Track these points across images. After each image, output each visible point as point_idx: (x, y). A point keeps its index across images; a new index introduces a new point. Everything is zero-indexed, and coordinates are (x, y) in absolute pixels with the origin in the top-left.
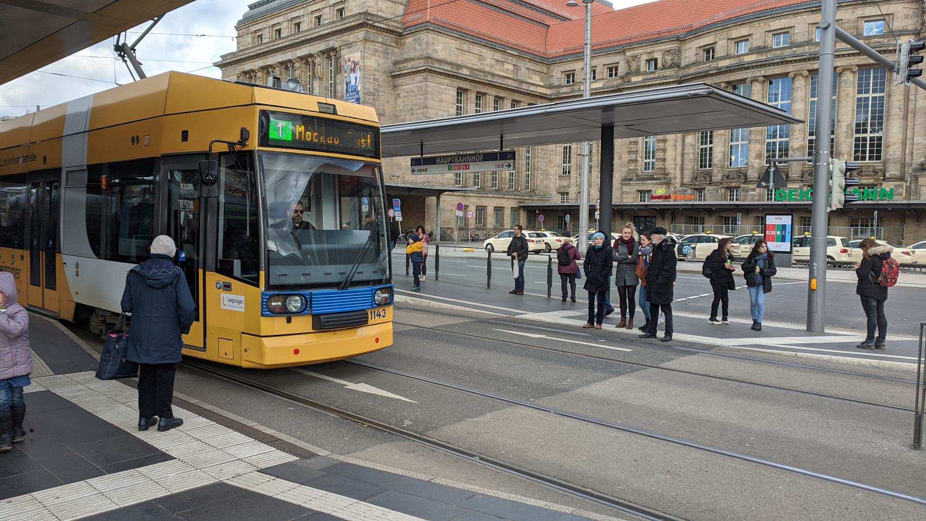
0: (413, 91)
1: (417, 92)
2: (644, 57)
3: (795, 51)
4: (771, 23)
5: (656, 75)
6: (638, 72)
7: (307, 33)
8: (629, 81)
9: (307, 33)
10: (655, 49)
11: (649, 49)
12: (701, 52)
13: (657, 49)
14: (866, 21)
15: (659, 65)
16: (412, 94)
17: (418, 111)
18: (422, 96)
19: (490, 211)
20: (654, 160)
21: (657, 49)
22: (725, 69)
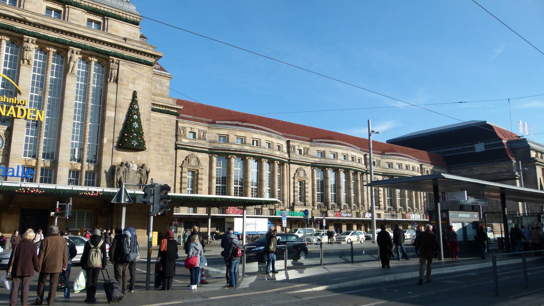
0: (160, 120)
1: (165, 122)
2: (188, 130)
3: (263, 150)
4: (253, 135)
5: (196, 141)
6: (185, 137)
7: (75, 27)
8: (181, 141)
9: (75, 27)
10: (195, 127)
11: (192, 126)
12: (218, 136)
13: (197, 127)
14: (331, 153)
15: (197, 137)
16: (160, 122)
17: (166, 137)
18: (171, 127)
19: (422, 218)
20: (188, 189)
21: (197, 127)
22: (239, 150)
